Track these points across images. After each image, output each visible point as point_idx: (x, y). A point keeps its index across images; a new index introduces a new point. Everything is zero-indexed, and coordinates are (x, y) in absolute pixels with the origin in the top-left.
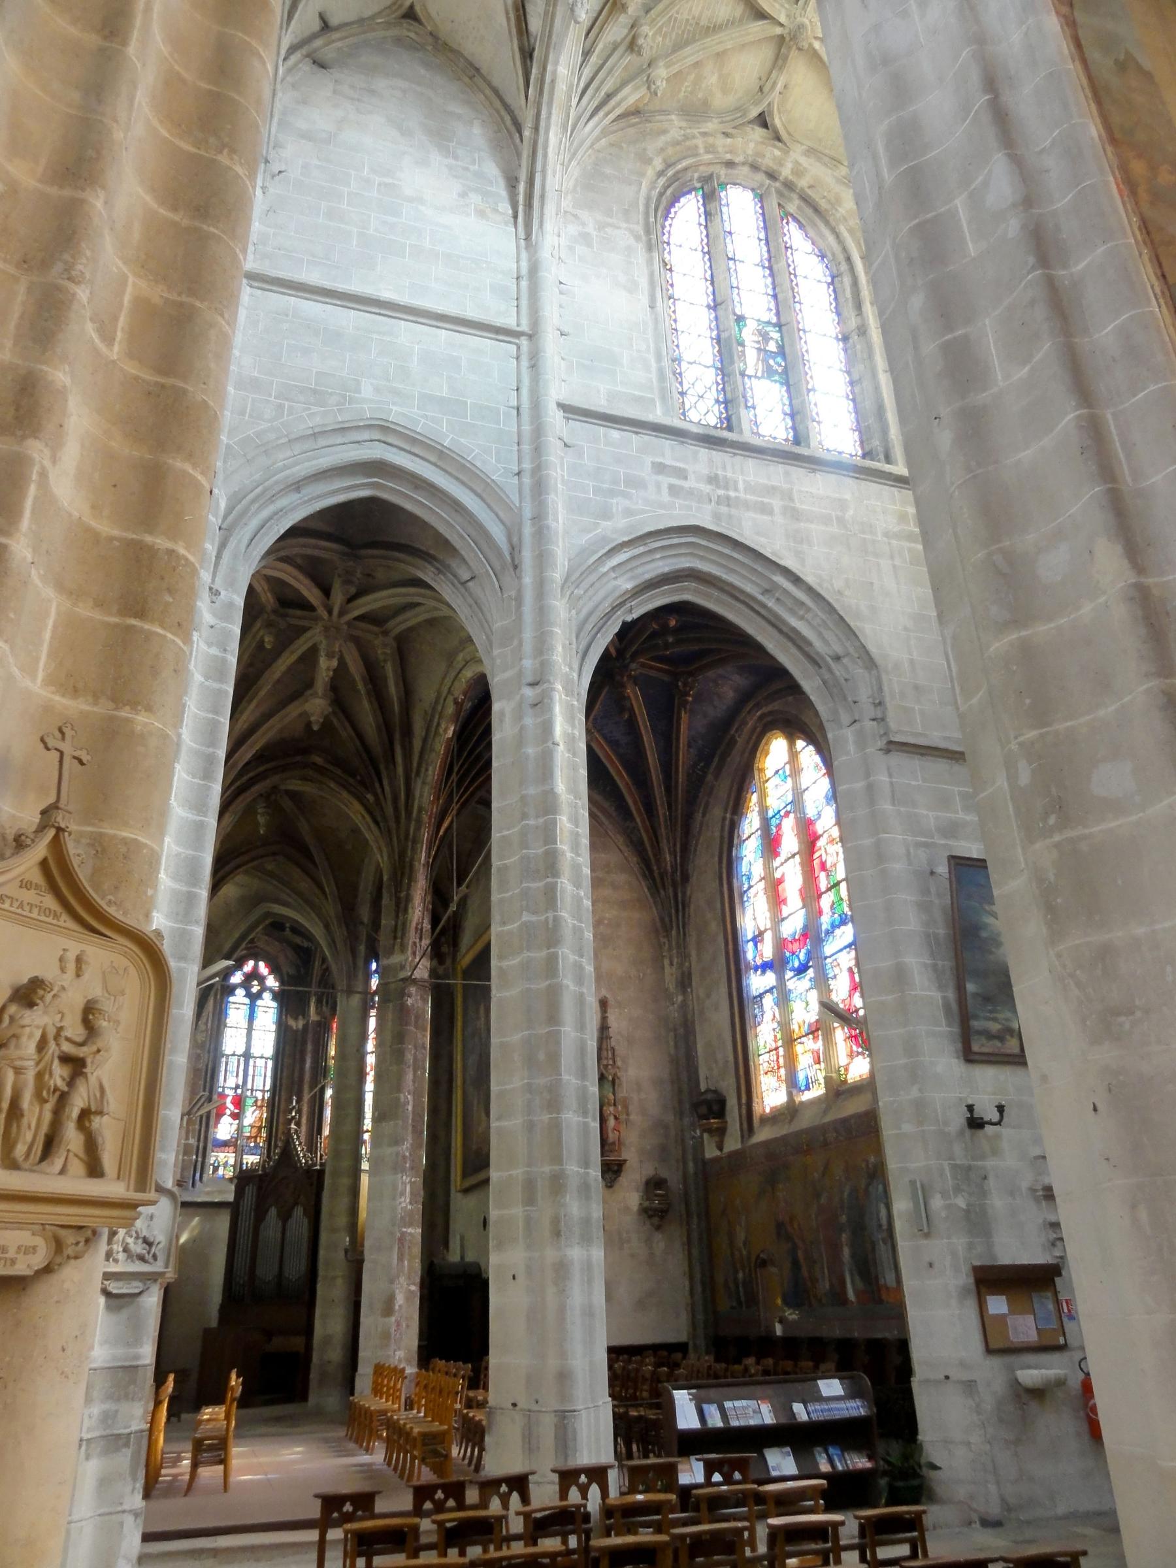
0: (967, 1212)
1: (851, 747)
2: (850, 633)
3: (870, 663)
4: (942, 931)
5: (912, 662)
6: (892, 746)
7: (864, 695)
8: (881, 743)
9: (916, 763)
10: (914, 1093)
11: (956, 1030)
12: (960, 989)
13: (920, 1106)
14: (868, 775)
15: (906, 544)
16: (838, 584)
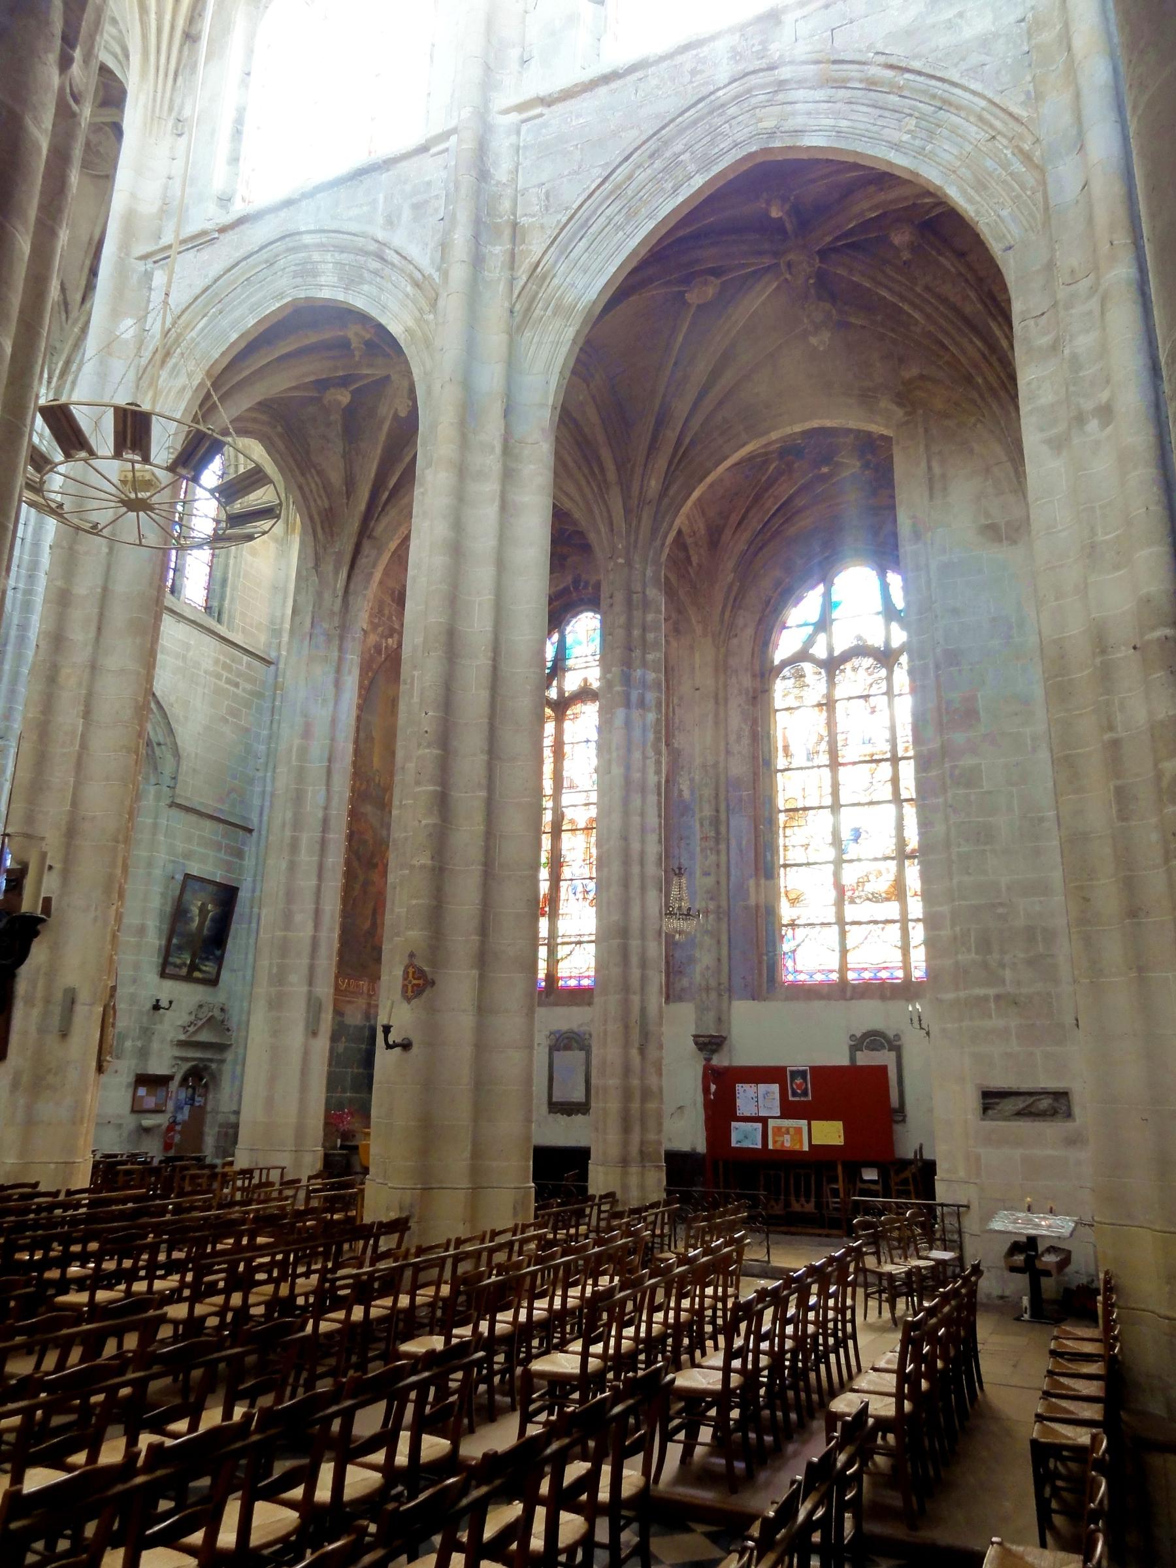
0: (141, 1048)
1: (151, 797)
2: (171, 732)
3: (177, 754)
4: (168, 909)
5: (196, 754)
6: (173, 805)
7: (168, 769)
8: (168, 801)
9: (182, 815)
10: (132, 990)
11: (161, 961)
12: (169, 940)
13: (133, 999)
14: (156, 817)
15: (214, 680)
16: (173, 699)
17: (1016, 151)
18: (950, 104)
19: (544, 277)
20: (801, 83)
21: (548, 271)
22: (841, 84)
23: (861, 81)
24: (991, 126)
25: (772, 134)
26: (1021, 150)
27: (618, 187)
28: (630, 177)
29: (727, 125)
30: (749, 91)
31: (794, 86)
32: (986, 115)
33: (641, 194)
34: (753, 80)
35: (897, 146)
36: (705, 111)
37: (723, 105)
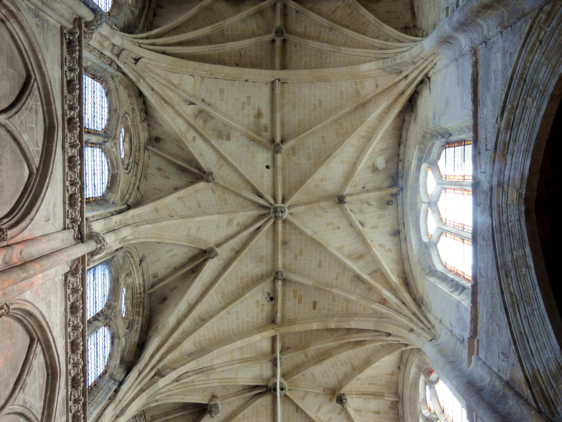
17: (547, 24)
18: (523, 74)
19: (535, 377)
20: (501, 172)
21: (534, 372)
22: (506, 146)
23: (506, 133)
24: (534, 44)
25: (520, 195)
26: (546, 21)
27: (513, 303)
28: (511, 294)
29: (510, 224)
30: (498, 206)
31: (502, 177)
32: (528, 49)
33: (522, 290)
34: (494, 202)
35: (538, 110)
36: (499, 235)
37: (500, 224)
